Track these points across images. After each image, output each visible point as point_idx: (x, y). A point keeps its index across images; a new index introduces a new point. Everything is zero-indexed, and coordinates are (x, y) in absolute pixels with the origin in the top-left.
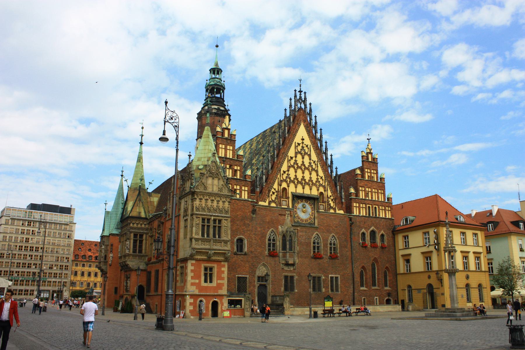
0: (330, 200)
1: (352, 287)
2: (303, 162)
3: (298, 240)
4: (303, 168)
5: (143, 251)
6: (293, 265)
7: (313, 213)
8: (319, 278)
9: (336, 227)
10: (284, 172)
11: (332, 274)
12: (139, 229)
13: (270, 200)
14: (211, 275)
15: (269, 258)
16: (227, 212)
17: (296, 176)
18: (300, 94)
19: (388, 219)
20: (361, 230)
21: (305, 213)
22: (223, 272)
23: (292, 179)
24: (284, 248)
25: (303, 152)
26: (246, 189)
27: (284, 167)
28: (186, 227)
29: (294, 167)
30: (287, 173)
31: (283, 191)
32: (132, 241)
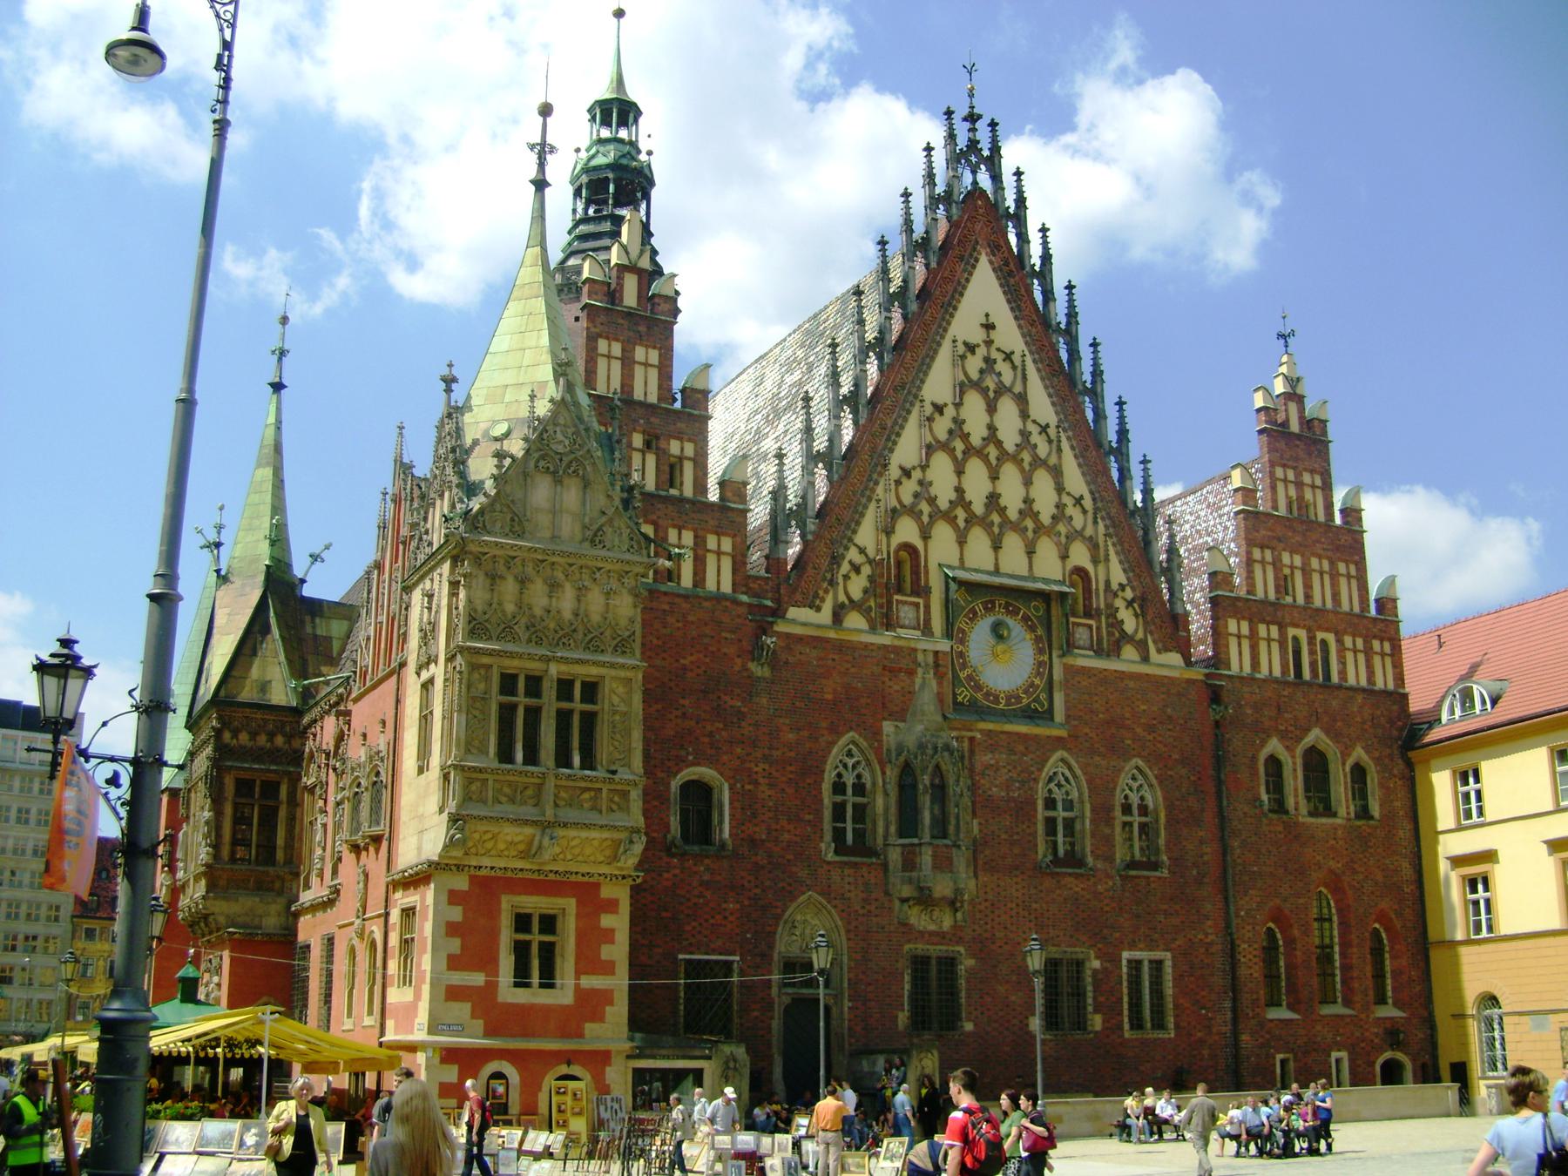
0: (1119, 603)
1: (1228, 1004)
2: (992, 428)
3: (974, 788)
4: (993, 452)
5: (280, 855)
6: (953, 904)
7: (1040, 664)
9: (1151, 729)
10: (907, 473)
11: (1132, 946)
12: (258, 755)
13: (842, 598)
14: (548, 952)
15: (835, 876)
16: (622, 646)
17: (959, 490)
18: (973, 130)
19: (1385, 692)
20: (1263, 743)
21: (1005, 664)
22: (608, 936)
23: (943, 504)
24: (908, 823)
25: (990, 383)
26: (727, 544)
27: (907, 450)
28: (425, 719)
29: (951, 452)
30: (917, 474)
31: (899, 564)
32: (228, 810)
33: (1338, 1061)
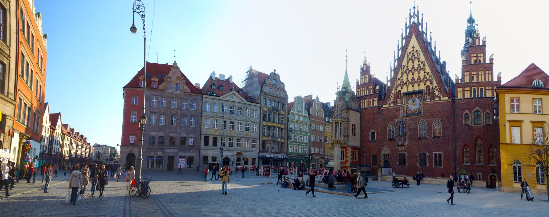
2: (413, 66)
8: (425, 155)
9: (439, 112)
17: (407, 79)
20: (464, 111)
21: (414, 105)
27: (399, 76)
33: (480, 175)
